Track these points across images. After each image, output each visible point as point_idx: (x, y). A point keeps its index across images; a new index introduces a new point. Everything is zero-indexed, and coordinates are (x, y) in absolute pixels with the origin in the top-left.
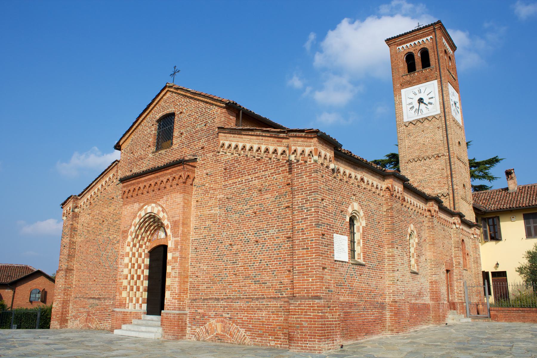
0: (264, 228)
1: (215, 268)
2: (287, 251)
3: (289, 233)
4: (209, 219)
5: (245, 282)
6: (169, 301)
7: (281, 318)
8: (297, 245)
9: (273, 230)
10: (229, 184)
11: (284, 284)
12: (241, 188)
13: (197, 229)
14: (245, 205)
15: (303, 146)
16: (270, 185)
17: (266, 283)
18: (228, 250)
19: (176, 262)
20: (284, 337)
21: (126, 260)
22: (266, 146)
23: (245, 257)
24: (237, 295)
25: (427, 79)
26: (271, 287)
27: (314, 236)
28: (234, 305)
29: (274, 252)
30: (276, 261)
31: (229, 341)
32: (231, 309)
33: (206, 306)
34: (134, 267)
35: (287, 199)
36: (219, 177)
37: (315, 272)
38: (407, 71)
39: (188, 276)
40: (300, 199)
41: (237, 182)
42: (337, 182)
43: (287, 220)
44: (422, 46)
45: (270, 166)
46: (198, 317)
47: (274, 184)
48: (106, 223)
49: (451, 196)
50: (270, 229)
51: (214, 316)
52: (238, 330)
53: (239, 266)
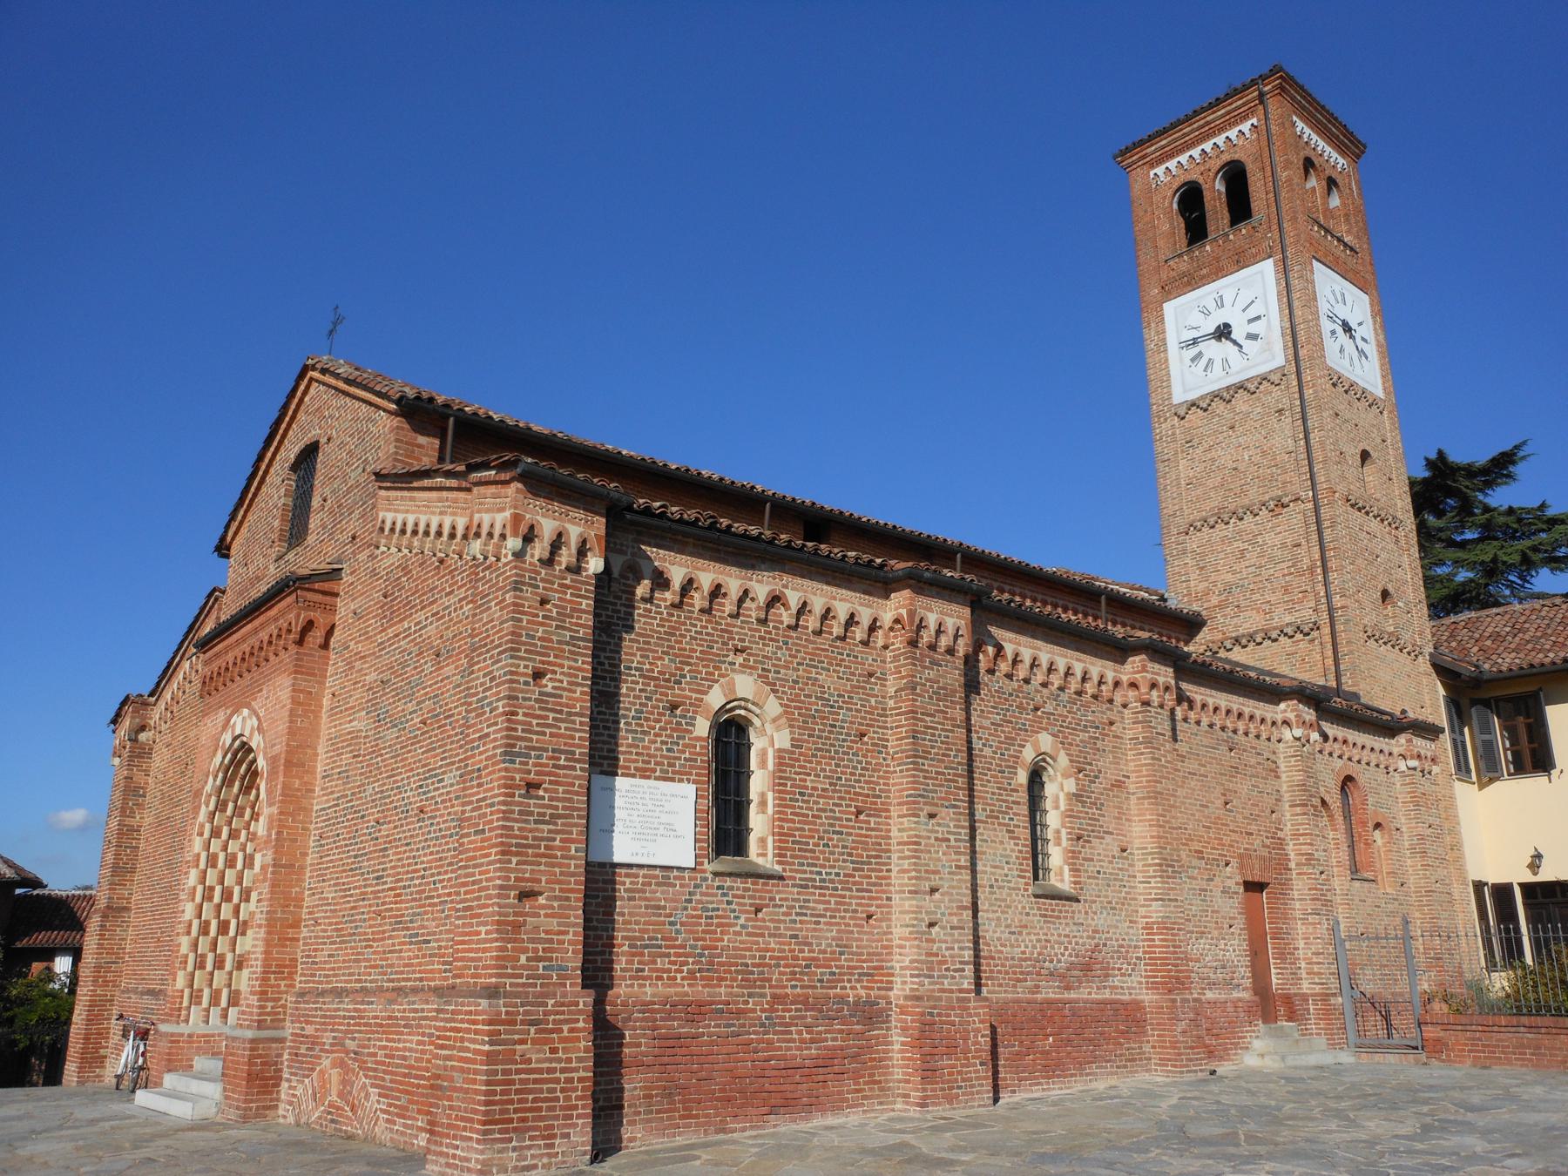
19: (264, 880)
25: (1241, 261)
34: (210, 899)
39: (300, 920)
42: (662, 613)
44: (1226, 158)
47: (461, 633)
49: (1326, 630)
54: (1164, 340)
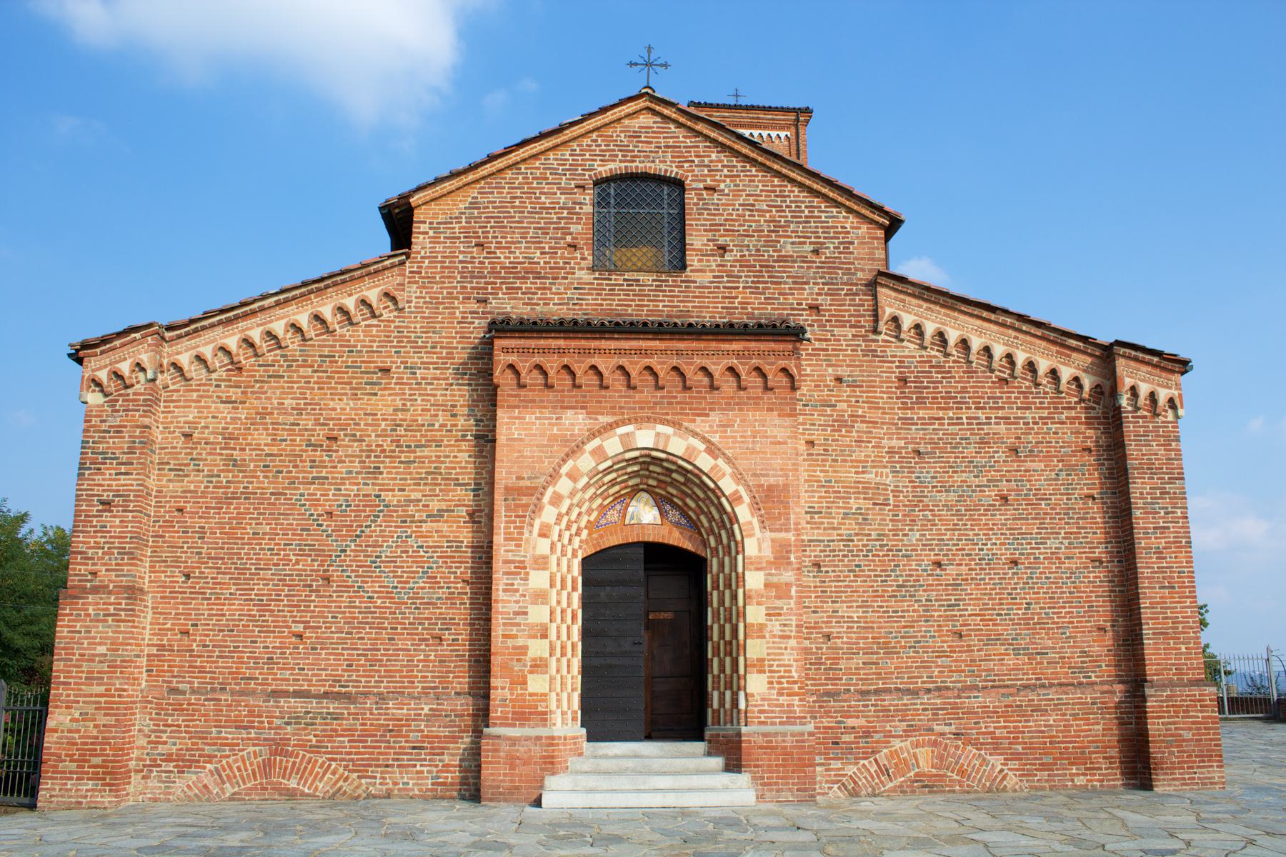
1: (889, 617)
2: (1093, 587)
3: (1097, 550)
4: (859, 493)
5: (986, 650)
6: (763, 700)
7: (1096, 727)
8: (1148, 578)
9: (1057, 541)
10: (918, 418)
11: (1092, 656)
12: (957, 434)
16: (1042, 442)
18: (929, 575)
20: (1108, 765)
22: (1028, 355)
23: (985, 594)
24: (966, 681)
26: (1058, 663)
28: (965, 702)
29: (1061, 588)
30: (1070, 607)
31: (958, 788)
32: (958, 713)
33: (873, 708)
35: (1086, 479)
36: (885, 396)
45: (1037, 400)
46: (846, 738)
50: (1049, 538)
51: (904, 731)
52: (984, 760)
53: (966, 613)
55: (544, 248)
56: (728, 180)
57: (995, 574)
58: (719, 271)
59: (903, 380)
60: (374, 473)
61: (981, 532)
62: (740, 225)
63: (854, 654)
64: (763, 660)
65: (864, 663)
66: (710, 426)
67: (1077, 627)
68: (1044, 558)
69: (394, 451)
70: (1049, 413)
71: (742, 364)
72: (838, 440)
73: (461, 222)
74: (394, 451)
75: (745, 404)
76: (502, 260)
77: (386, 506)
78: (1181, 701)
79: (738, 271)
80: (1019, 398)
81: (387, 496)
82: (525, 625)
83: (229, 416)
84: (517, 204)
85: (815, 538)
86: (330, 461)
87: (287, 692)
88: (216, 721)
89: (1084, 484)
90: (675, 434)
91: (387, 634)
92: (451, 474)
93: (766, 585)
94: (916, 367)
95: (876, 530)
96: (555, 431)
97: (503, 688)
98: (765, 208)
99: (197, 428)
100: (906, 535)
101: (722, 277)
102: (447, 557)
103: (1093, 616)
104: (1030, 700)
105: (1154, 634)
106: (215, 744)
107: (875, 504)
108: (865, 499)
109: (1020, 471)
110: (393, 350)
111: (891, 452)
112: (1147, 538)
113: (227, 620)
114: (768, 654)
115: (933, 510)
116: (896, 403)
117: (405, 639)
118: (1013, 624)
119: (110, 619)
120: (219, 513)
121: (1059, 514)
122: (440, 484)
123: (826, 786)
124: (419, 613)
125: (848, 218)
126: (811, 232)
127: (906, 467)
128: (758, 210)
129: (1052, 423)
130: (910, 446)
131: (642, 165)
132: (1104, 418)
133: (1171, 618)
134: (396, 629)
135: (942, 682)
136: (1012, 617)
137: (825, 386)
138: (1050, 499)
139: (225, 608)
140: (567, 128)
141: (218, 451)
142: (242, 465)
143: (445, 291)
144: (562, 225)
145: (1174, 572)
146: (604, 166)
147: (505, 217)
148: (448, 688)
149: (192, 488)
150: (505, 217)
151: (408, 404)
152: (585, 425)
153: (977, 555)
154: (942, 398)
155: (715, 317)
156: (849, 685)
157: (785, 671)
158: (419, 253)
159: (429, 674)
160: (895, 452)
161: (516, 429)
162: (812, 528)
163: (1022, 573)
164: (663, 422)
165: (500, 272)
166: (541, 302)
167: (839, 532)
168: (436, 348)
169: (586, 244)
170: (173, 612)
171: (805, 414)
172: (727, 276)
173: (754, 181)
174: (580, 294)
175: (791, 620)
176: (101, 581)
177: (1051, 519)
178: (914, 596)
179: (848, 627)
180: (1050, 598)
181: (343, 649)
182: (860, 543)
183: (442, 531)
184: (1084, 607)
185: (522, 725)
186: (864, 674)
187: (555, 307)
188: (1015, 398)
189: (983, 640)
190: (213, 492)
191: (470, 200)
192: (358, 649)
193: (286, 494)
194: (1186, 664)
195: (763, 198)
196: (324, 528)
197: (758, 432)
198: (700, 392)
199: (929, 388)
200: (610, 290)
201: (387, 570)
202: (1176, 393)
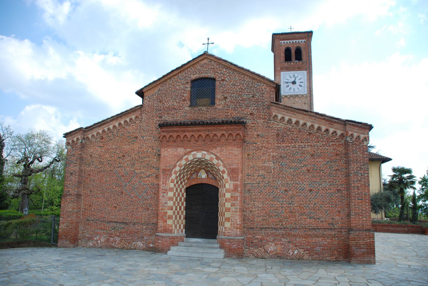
0: (317, 181)
1: (270, 206)
2: (337, 198)
3: (339, 187)
4: (262, 169)
6: (229, 229)
7: (335, 242)
8: (353, 196)
9: (326, 184)
10: (282, 146)
11: (336, 220)
12: (294, 151)
13: (249, 175)
14: (299, 164)
15: (359, 133)
16: (322, 153)
17: (320, 219)
18: (283, 194)
21: (171, 194)
22: (318, 125)
23: (301, 200)
25: (299, 69)
26: (324, 222)
27: (367, 192)
29: (326, 198)
30: (329, 205)
33: (264, 233)
35: (337, 164)
36: (272, 140)
37: (368, 215)
38: (284, 60)
40: (355, 167)
41: (290, 146)
43: (338, 178)
44: (298, 45)
45: (322, 139)
46: (255, 241)
48: (128, 158)
50: (323, 183)
53: (295, 206)
54: (280, 80)
55: (177, 101)
56: (228, 77)
57: (304, 194)
58: (224, 105)
59: (278, 135)
60: (133, 165)
61: (301, 181)
62: (231, 91)
63: (259, 217)
64: (229, 218)
65: (262, 220)
66: (217, 151)
67: (331, 211)
68: (321, 189)
69: (138, 159)
70: (325, 143)
71: (226, 133)
72: (257, 154)
73: (156, 95)
74: (138, 159)
75: (227, 144)
76: (166, 105)
77: (136, 174)
78: (362, 236)
79: (230, 104)
80: (315, 139)
81: (136, 171)
82: (167, 206)
83: (100, 150)
84: (170, 89)
85: (249, 183)
86: (123, 162)
87: (113, 221)
88: (97, 228)
89: (336, 166)
90: (207, 154)
91: (136, 207)
92: (152, 165)
93: (231, 197)
94: (282, 130)
95: (267, 180)
96: (176, 154)
97: (161, 223)
98: (239, 84)
99: (93, 154)
100: (277, 182)
101: (225, 106)
102: (151, 187)
103: (337, 207)
104: (313, 233)
105: (354, 214)
106: (96, 234)
107: (267, 173)
108: (264, 171)
109: (315, 162)
110: (139, 132)
111: (273, 157)
112: (354, 183)
113: (100, 203)
114: (231, 216)
115: (286, 174)
116: (275, 142)
117: (140, 209)
118: (309, 209)
119: (72, 202)
120: (98, 176)
121: (327, 175)
122: (149, 168)
123: (249, 254)
124: (144, 202)
125: (263, 85)
126: (252, 91)
127: (278, 161)
128: (236, 86)
129: (326, 146)
130: (279, 155)
131: (204, 75)
132: (344, 144)
133: (361, 209)
134: (138, 206)
135: (286, 226)
136: (309, 207)
137: (254, 137)
138: (324, 171)
139: (99, 199)
140: (183, 66)
141: (98, 159)
142: (103, 163)
143: (151, 115)
144: (182, 94)
145: (363, 194)
146: (194, 76)
147: (167, 93)
148: (150, 222)
149: (92, 169)
150: (167, 93)
151: (142, 146)
152: (183, 152)
153: (299, 188)
154: (290, 140)
155: (223, 119)
156: (257, 226)
157: (236, 221)
158: (145, 105)
159: (146, 218)
160: (274, 157)
161: (166, 153)
162: (248, 180)
163: (313, 194)
164: (204, 150)
165: (165, 109)
166: (176, 117)
167: (256, 181)
168: (149, 131)
169: (188, 99)
170: (88, 200)
171: (247, 146)
172: (227, 106)
173: (236, 77)
174: (186, 114)
175: (238, 207)
176: (71, 193)
177: (324, 177)
178: (278, 200)
179: (258, 209)
180: (322, 201)
181: (126, 211)
182: (262, 184)
183: (149, 180)
184: (334, 205)
185: (165, 233)
186: (262, 223)
187: (179, 117)
188: (314, 139)
189: (299, 214)
190: (96, 170)
191: (158, 89)
192: (129, 211)
193: (113, 171)
194: (365, 224)
195: (238, 82)
196: (122, 179)
197: (230, 152)
198: (215, 141)
199: (286, 137)
200: (194, 112)
201: (136, 190)
202: (367, 136)
